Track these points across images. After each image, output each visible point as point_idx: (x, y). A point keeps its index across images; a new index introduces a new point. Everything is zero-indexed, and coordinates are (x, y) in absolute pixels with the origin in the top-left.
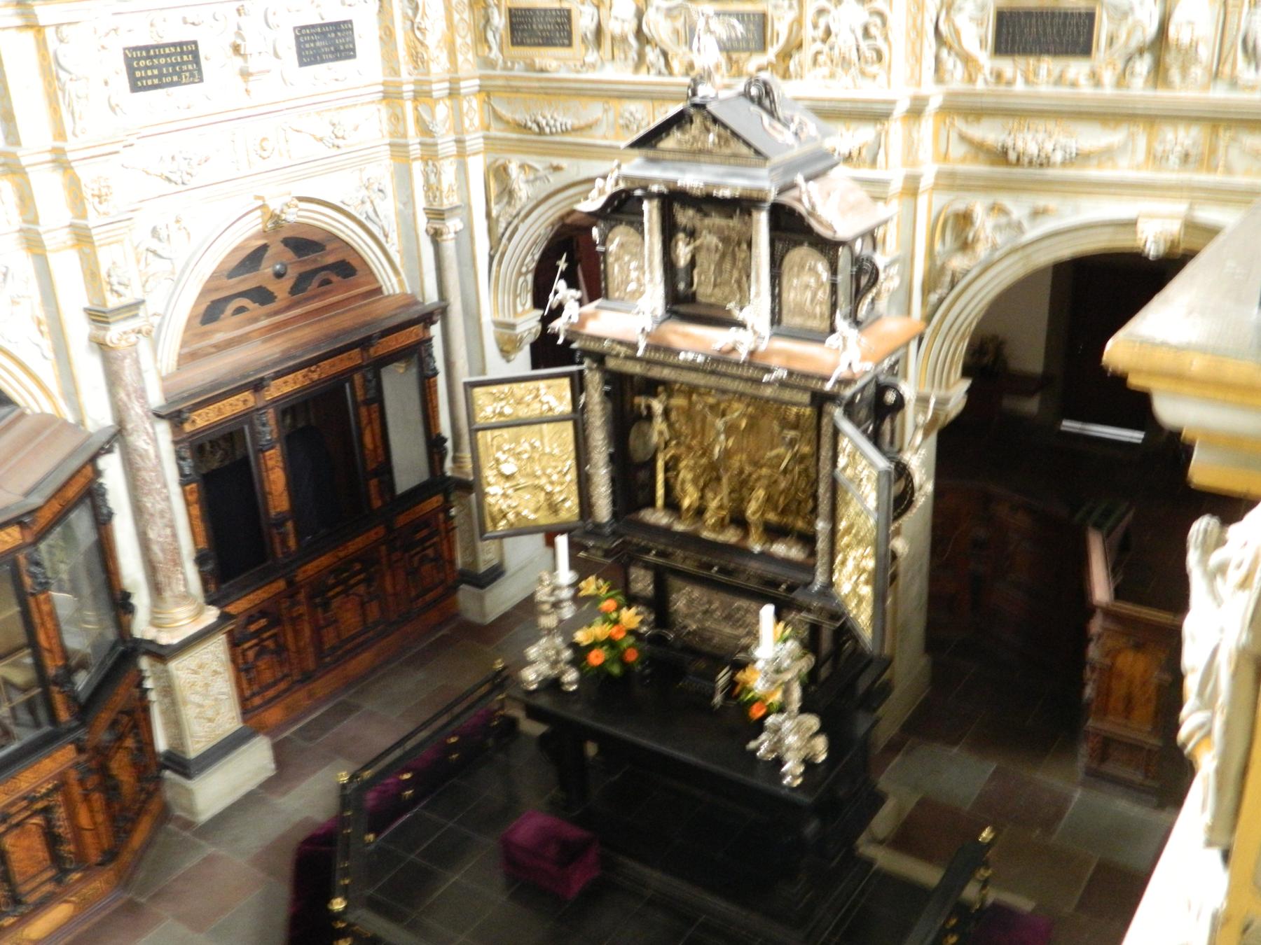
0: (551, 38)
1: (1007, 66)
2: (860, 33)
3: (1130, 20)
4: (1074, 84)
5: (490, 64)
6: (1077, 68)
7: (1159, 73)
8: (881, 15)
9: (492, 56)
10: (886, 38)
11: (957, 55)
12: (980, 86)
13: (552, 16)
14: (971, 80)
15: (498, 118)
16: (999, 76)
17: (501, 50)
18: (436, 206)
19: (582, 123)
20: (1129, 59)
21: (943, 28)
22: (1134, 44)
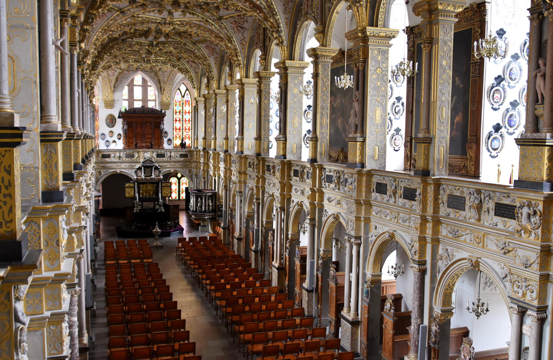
6: (164, 159)
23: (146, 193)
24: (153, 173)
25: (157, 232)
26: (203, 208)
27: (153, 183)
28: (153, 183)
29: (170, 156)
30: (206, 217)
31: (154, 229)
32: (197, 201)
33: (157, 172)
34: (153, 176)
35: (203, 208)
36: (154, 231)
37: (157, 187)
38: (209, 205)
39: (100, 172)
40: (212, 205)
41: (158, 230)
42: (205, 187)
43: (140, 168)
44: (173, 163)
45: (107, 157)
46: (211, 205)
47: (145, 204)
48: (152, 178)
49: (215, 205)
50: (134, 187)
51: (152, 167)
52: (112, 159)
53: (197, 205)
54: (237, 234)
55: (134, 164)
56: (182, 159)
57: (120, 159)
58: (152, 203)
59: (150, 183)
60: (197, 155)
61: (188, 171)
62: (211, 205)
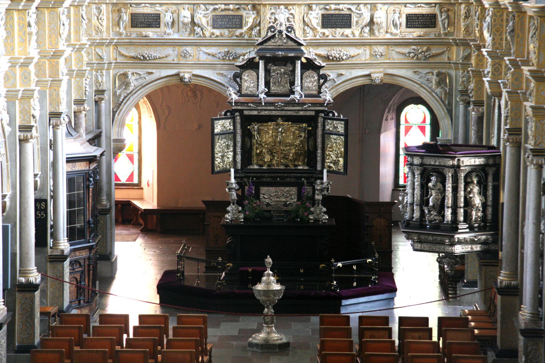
0: (150, 24)
1: (327, 31)
2: (286, 20)
3: (362, 17)
4: (347, 36)
5: (121, 34)
6: (347, 31)
7: (372, 31)
8: (292, 14)
9: (121, 31)
10: (294, 22)
11: (311, 28)
12: (318, 37)
13: (152, 16)
14: (315, 36)
15: (123, 55)
16: (324, 34)
17: (125, 28)
18: (100, 88)
19: (164, 55)
20: (363, 28)
21: (306, 19)
22: (364, 24)
23: (271, 153)
24: (298, 81)
25: (267, 292)
26: (448, 213)
27: (295, 119)
28: (295, 119)
29: (372, 22)
30: (458, 249)
31: (259, 281)
32: (425, 190)
33: (311, 81)
34: (297, 96)
35: (448, 213)
36: (260, 287)
37: (312, 135)
38: (468, 203)
39: (125, 75)
40: (484, 205)
41: (270, 284)
42: (480, 138)
43: (251, 65)
44: (380, 49)
45: (149, 26)
46: (477, 200)
47: (271, 196)
48: (293, 103)
49: (494, 206)
50: (234, 133)
51: (292, 61)
52: (166, 32)
53: (424, 202)
54: (525, 312)
55: (239, 51)
56: (416, 33)
57: (193, 31)
58: (294, 190)
59: (287, 118)
60: (467, 16)
61: (434, 79)
62: (477, 200)
